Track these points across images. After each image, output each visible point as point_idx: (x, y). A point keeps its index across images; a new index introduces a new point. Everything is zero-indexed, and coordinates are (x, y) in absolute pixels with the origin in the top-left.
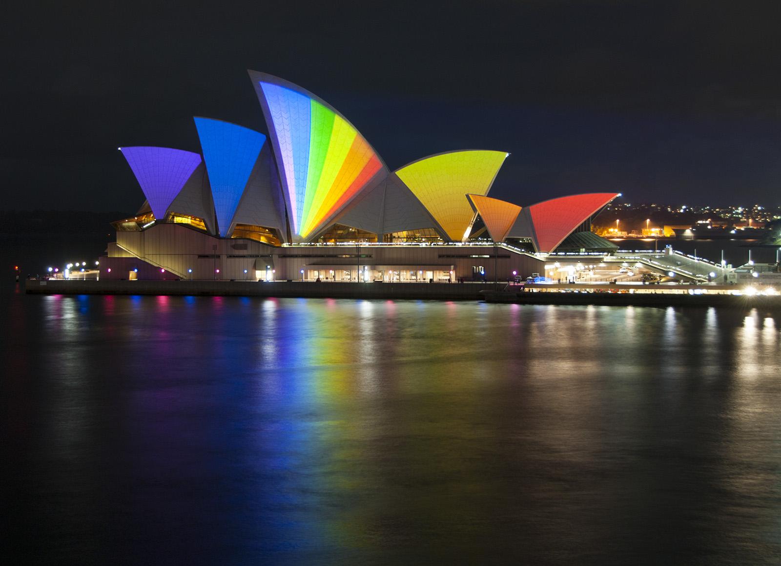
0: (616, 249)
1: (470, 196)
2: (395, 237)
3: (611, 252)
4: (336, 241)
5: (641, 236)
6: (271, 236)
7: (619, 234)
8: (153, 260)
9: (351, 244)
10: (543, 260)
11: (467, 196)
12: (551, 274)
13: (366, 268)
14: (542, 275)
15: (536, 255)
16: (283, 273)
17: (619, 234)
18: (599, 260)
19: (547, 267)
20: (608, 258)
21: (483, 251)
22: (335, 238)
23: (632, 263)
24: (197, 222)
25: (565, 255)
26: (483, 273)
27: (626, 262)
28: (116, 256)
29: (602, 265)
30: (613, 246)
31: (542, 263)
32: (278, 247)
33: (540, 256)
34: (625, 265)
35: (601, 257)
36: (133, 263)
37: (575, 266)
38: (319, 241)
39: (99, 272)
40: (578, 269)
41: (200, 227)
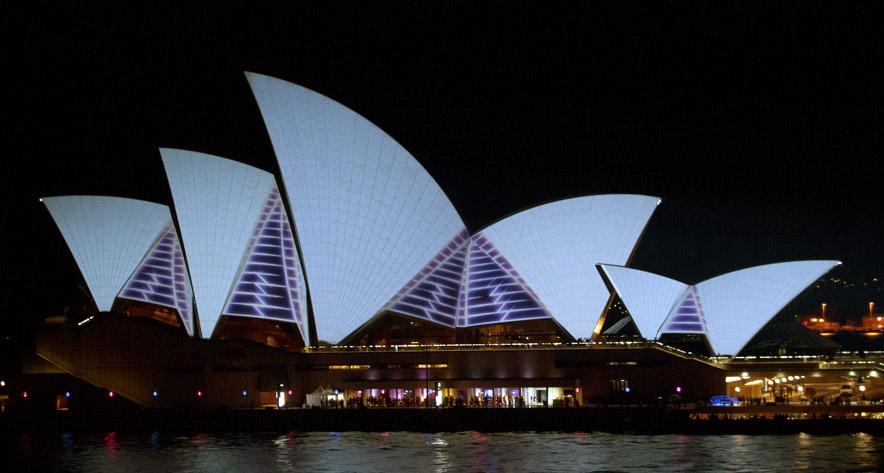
0: (836, 349)
1: (603, 266)
2: (483, 335)
3: (830, 354)
4: (388, 345)
5: (861, 329)
6: (284, 335)
7: (827, 326)
8: (95, 377)
9: (414, 345)
10: (722, 368)
11: (599, 268)
12: (737, 389)
13: (439, 385)
14: (722, 389)
15: (711, 361)
16: (297, 400)
17: (827, 326)
18: (813, 367)
19: (729, 379)
20: (823, 365)
21: (627, 354)
22: (386, 339)
23: (863, 371)
24: (165, 315)
25: (758, 359)
26: (628, 390)
27: (854, 370)
28: (36, 372)
29: (817, 375)
30: (833, 344)
31: (723, 373)
32: (293, 354)
33: (715, 362)
34: (852, 374)
35: (814, 362)
36: (62, 382)
37: (770, 377)
38: (362, 341)
39: (6, 397)
40: (777, 381)
41: (171, 323)
